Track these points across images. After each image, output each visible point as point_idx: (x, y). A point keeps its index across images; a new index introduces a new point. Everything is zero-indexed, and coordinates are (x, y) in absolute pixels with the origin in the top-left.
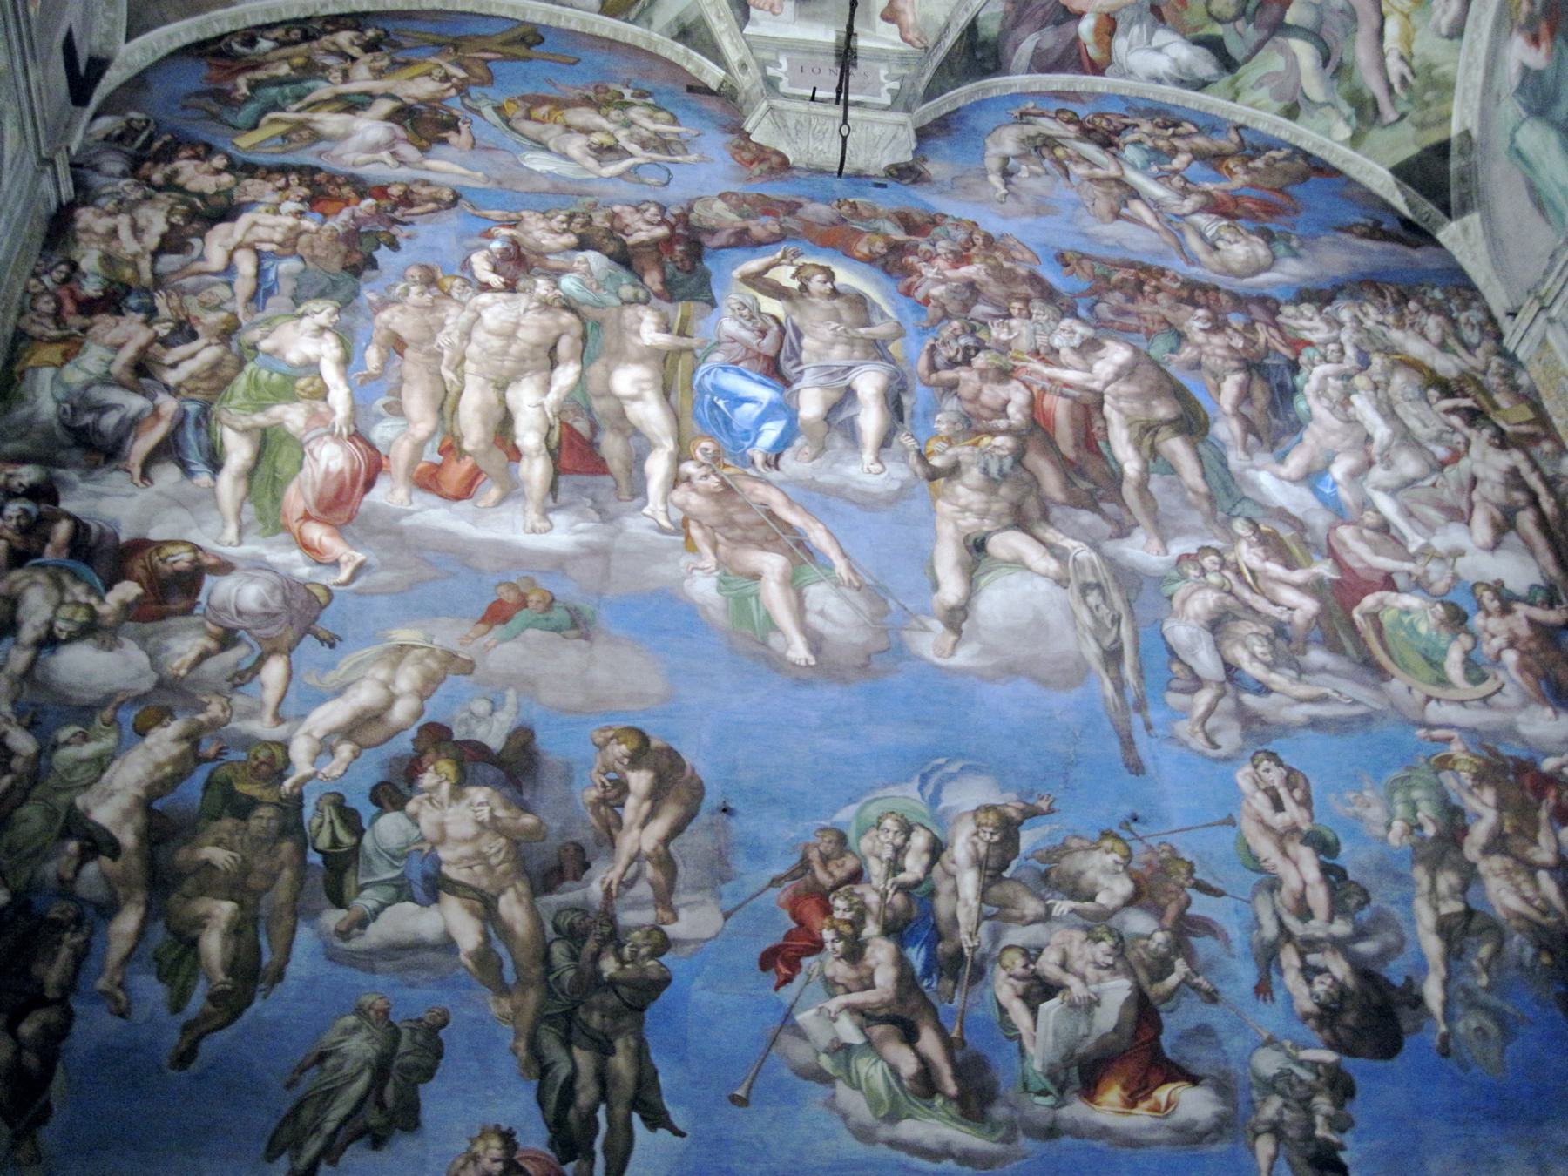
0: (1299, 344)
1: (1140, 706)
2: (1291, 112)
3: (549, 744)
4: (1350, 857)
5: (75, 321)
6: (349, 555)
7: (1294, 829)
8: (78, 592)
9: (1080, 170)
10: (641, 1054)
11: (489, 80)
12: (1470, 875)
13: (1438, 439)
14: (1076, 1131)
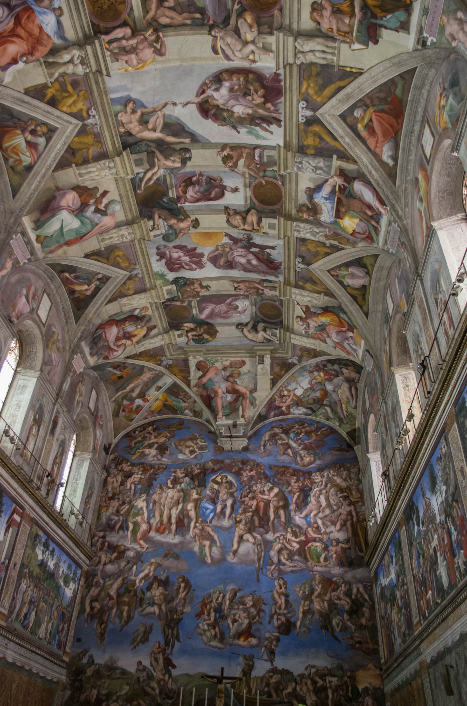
0: (313, 483)
1: (262, 569)
2: (328, 419)
3: (171, 579)
4: (291, 598)
5: (108, 502)
6: (146, 546)
7: (282, 593)
8: (109, 555)
9: (280, 442)
10: (178, 631)
11: (173, 436)
12: (311, 602)
13: (335, 505)
14: (235, 645)
